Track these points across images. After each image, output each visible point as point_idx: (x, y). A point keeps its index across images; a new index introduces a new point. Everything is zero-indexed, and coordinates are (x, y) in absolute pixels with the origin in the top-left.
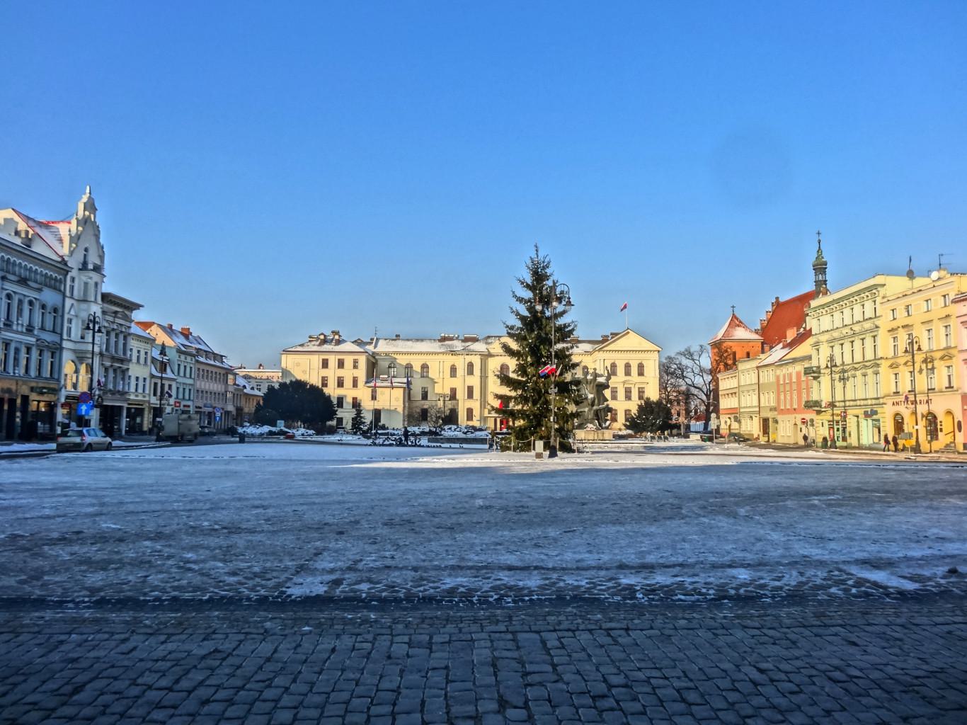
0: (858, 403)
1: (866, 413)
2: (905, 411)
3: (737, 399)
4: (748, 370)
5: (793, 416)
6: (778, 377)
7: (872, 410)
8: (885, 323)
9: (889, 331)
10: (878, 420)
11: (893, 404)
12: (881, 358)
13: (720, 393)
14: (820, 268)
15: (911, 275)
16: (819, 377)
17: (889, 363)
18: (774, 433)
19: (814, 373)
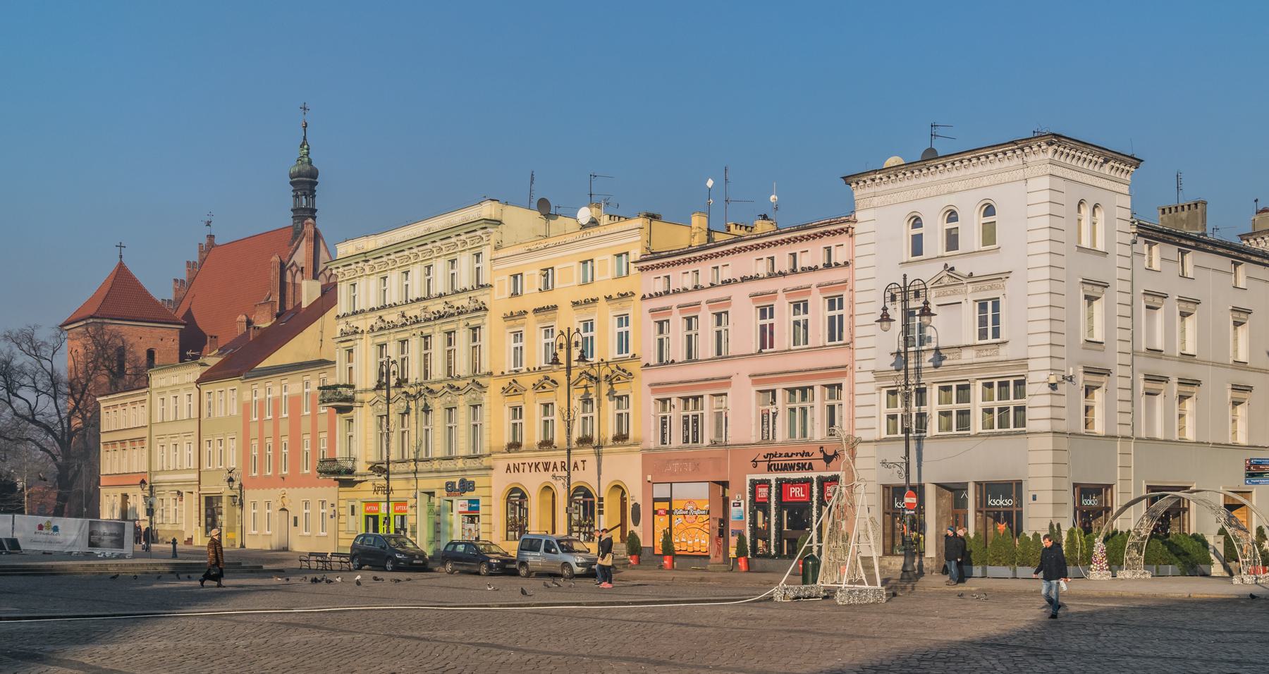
0: (436, 465)
1: (450, 488)
2: (532, 483)
3: (146, 451)
4: (175, 388)
5: (279, 491)
6: (246, 408)
7: (463, 482)
8: (498, 299)
9: (506, 318)
10: (477, 501)
11: (508, 468)
12: (490, 374)
13: (104, 438)
14: (305, 182)
15: (546, 209)
16: (349, 409)
17: (505, 382)
18: (231, 529)
19: (340, 400)
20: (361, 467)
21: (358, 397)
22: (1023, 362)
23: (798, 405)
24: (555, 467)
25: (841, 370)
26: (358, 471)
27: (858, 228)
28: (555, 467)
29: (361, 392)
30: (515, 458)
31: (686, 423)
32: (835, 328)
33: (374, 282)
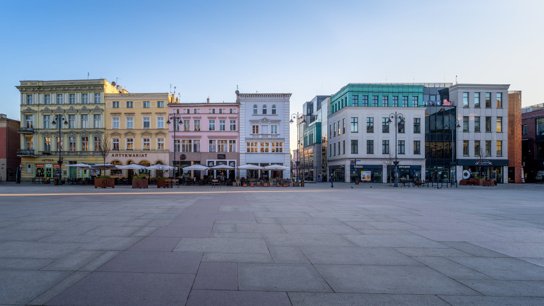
9: (111, 114)
11: (113, 155)
20: (36, 153)
21: (35, 131)
22: (283, 139)
23: (221, 144)
24: (134, 155)
25: (235, 137)
26: (35, 154)
27: (240, 106)
28: (134, 155)
29: (36, 129)
30: (115, 152)
31: (183, 146)
32: (233, 128)
33: (42, 96)
